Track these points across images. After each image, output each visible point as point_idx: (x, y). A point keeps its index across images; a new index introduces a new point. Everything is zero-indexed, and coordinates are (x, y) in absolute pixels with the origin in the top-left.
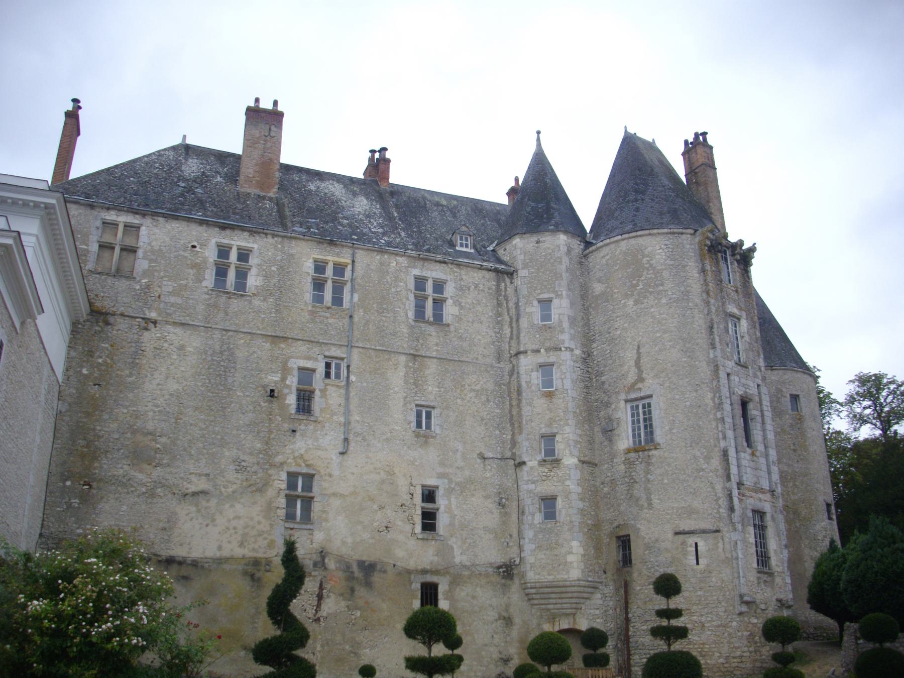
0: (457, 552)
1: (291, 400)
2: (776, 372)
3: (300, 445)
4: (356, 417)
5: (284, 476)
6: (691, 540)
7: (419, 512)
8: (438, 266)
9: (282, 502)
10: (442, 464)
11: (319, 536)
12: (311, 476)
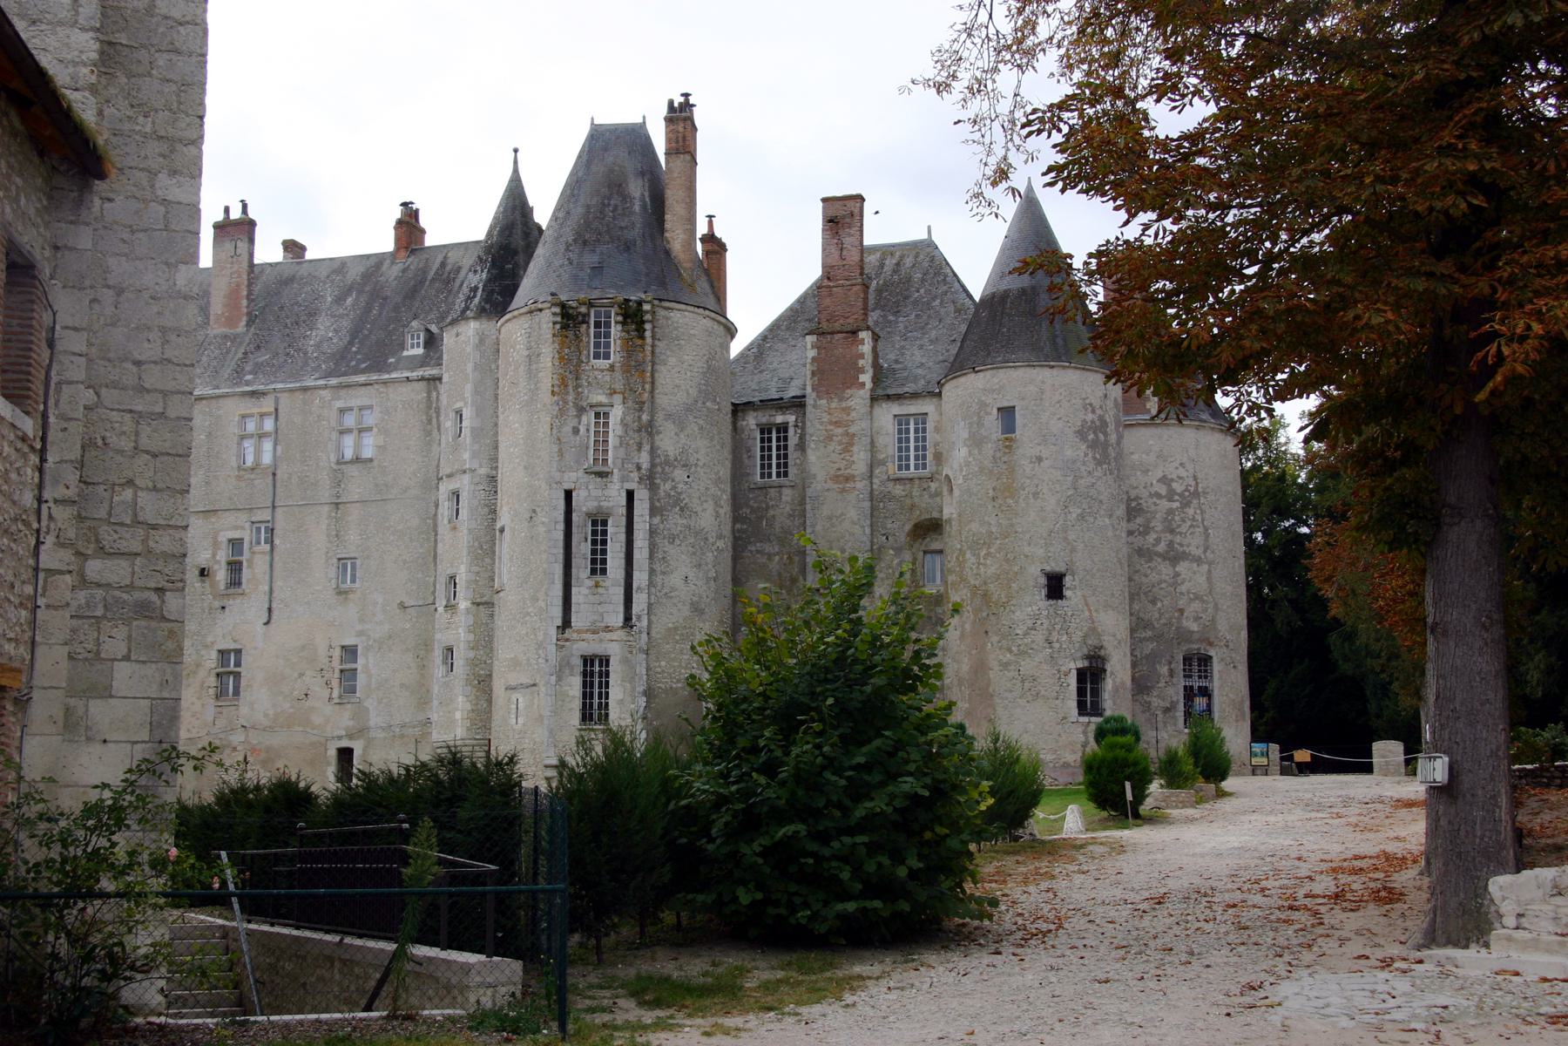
0: (372, 714)
1: (221, 575)
2: (981, 375)
3: (228, 621)
4: (278, 584)
5: (214, 655)
6: (514, 696)
7: (337, 675)
8: (363, 390)
9: (213, 681)
10: (361, 620)
11: (244, 710)
12: (238, 652)
